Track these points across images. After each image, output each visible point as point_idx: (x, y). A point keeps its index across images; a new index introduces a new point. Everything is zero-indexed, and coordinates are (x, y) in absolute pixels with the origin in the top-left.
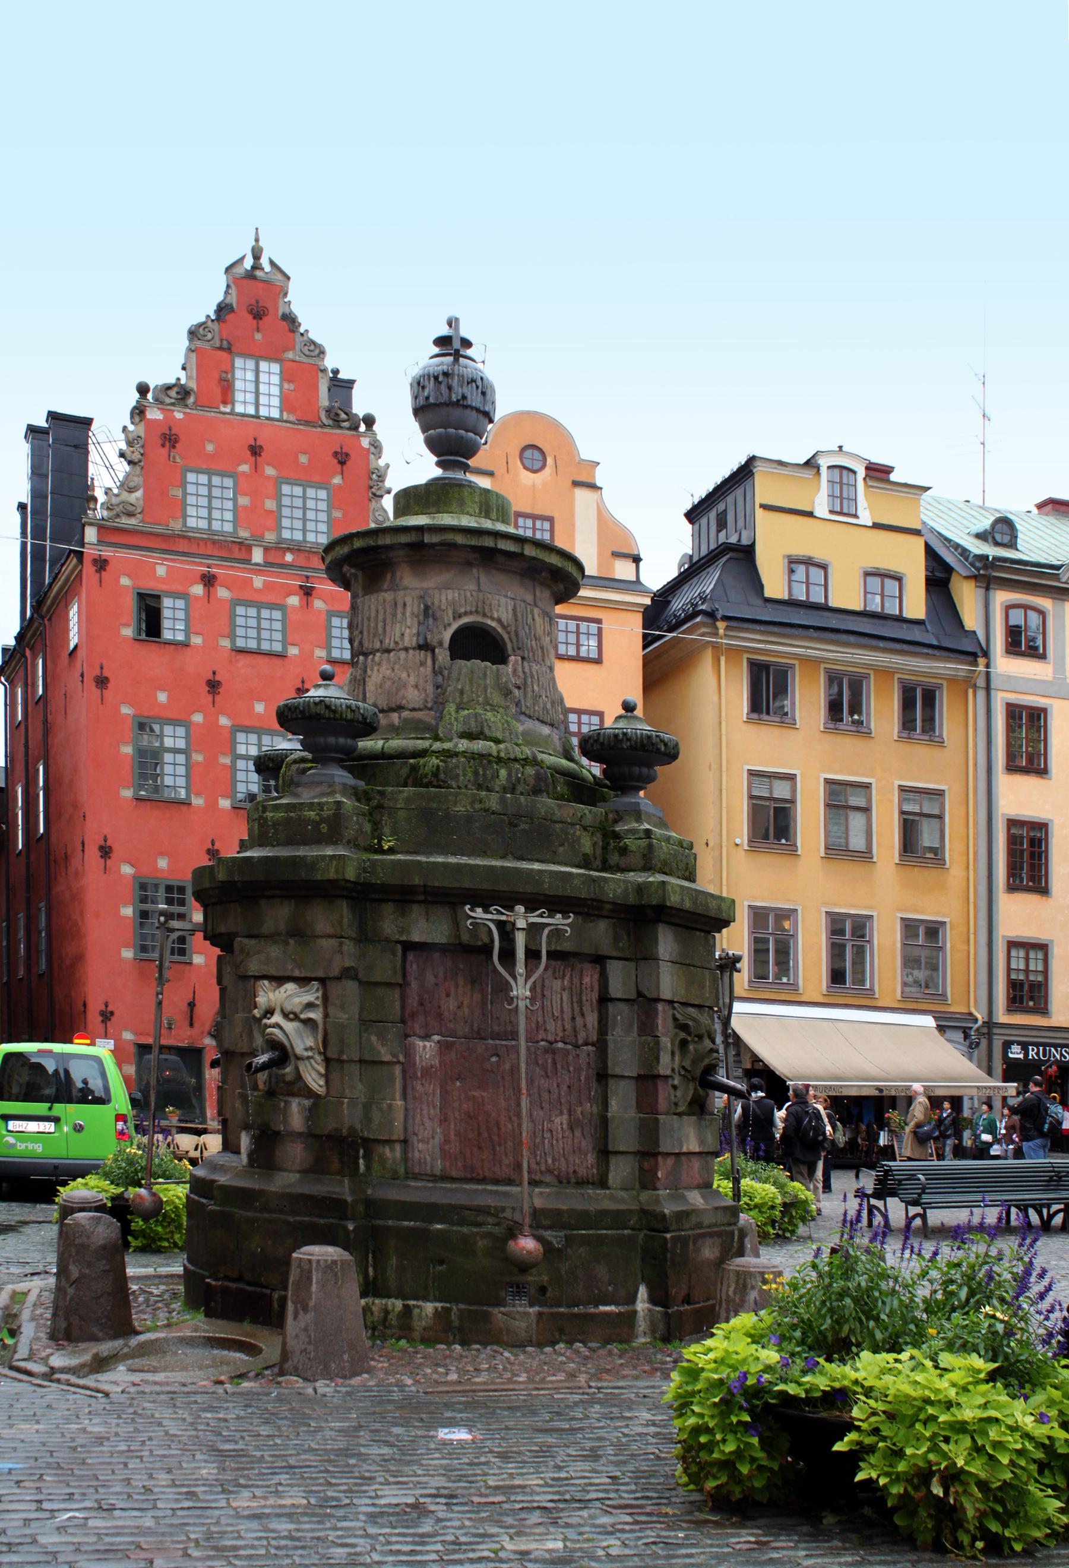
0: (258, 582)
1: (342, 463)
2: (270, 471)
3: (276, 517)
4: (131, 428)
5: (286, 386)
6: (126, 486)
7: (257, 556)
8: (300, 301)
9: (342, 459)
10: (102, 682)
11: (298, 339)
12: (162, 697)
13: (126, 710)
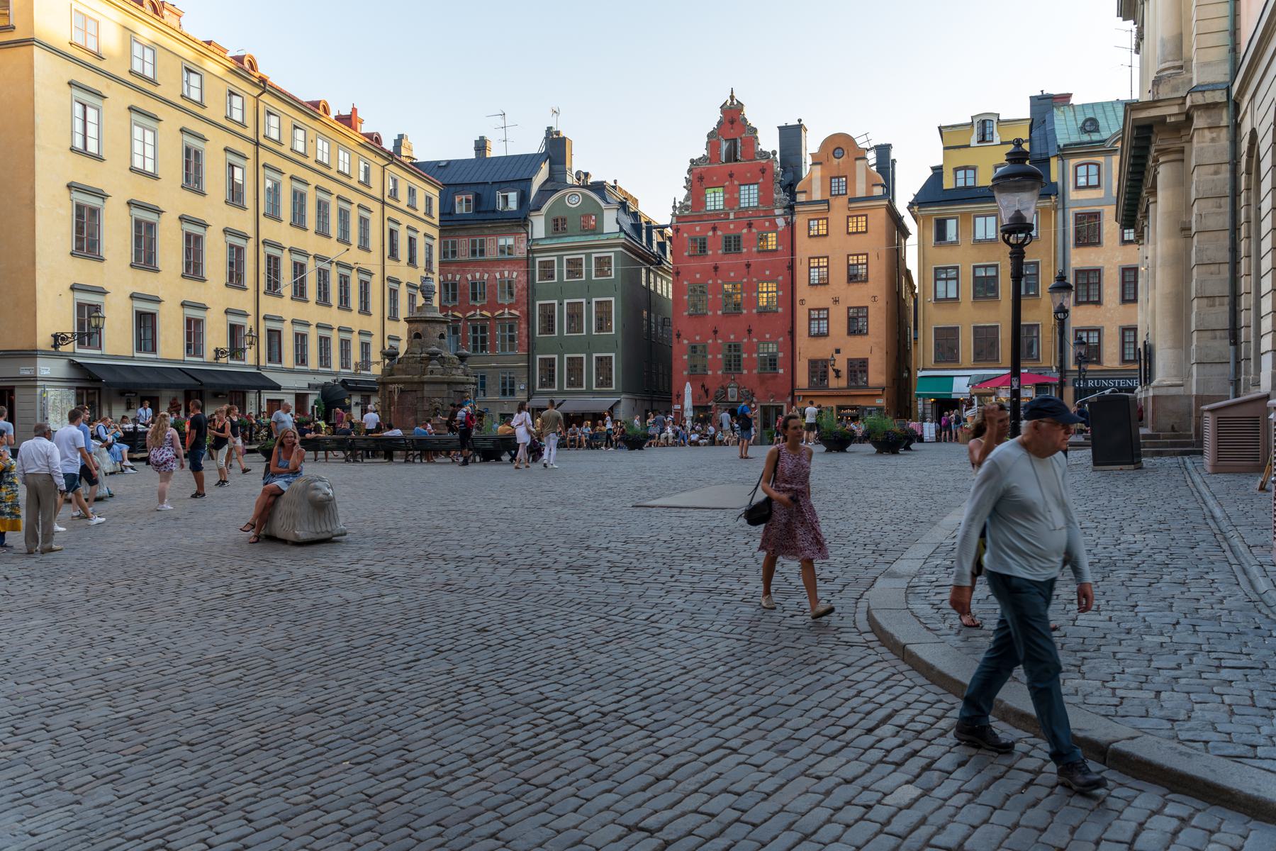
7: (732, 216)
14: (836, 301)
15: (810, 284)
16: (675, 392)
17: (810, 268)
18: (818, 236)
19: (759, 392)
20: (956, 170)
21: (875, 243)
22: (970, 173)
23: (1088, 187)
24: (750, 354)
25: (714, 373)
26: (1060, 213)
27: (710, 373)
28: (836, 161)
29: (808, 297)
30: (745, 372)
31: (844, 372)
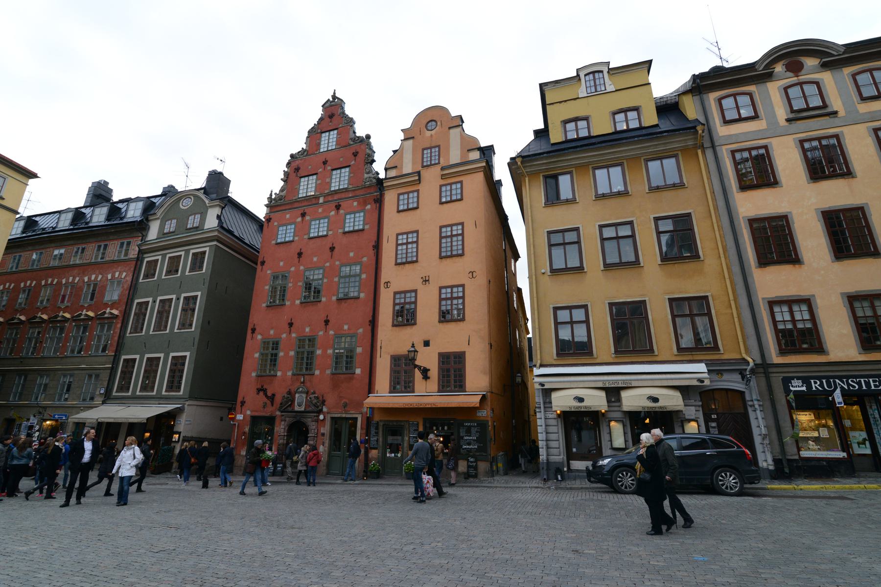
0: (320, 210)
1: (355, 156)
3: (330, 183)
4: (286, 170)
6: (282, 190)
7: (321, 200)
9: (355, 154)
10: (263, 263)
12: (281, 264)
14: (426, 281)
15: (397, 264)
16: (240, 399)
18: (408, 210)
19: (331, 399)
20: (565, 122)
21: (471, 210)
22: (582, 124)
23: (740, 120)
24: (325, 351)
25: (284, 374)
26: (709, 153)
27: (279, 374)
28: (428, 133)
29: (395, 279)
30: (317, 372)
31: (434, 373)
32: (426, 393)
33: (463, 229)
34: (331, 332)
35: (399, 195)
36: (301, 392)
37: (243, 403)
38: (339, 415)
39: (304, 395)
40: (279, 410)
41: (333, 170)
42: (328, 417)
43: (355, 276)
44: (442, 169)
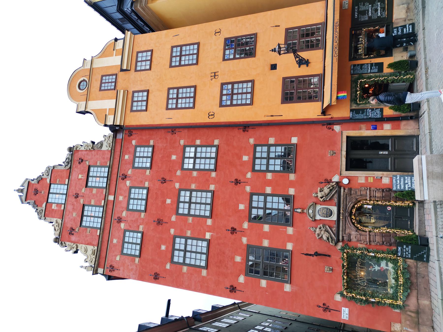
0: (121, 198)
2: (83, 190)
5: (58, 182)
8: (34, 175)
11: (43, 177)
13: (168, 266)
14: (215, 75)
17: (177, 108)
29: (208, 108)
32: (323, 62)
33: (177, 46)
34: (249, 175)
35: (132, 111)
36: (314, 212)
37: (326, 309)
38: (344, 160)
39: (319, 207)
40: (336, 244)
41: (86, 186)
42: (345, 173)
43: (196, 152)
44: (122, 70)
